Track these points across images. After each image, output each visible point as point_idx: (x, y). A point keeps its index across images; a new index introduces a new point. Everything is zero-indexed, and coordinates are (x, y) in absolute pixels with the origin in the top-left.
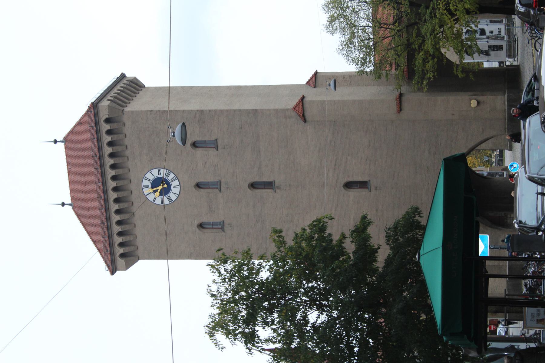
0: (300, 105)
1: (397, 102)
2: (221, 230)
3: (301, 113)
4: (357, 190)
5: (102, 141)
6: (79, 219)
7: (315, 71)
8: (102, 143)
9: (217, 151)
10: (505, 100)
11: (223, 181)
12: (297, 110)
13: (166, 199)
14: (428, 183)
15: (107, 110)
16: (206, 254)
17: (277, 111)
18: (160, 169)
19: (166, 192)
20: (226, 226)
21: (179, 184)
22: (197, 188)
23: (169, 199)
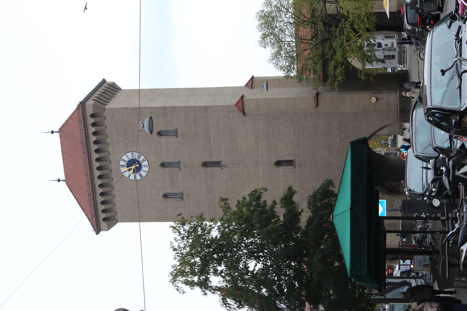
0: (241, 102)
1: (315, 100)
2: (180, 199)
4: (284, 167)
6: (72, 192)
7: (252, 76)
8: (89, 133)
9: (177, 138)
12: (238, 106)
14: (339, 161)
17: (222, 107)
18: (133, 152)
19: (138, 170)
20: (185, 196)
21: (148, 164)
22: (162, 167)
23: (141, 175)
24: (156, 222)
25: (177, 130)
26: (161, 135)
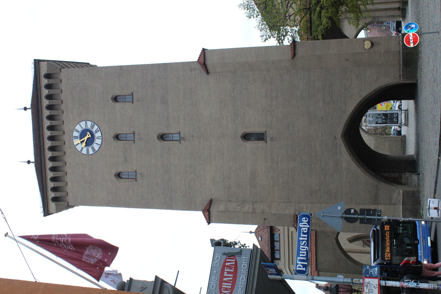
1: (291, 48)
2: (134, 180)
3: (202, 62)
4: (254, 142)
5: (41, 94)
8: (42, 96)
10: (400, 40)
13: (90, 149)
14: (322, 134)
15: (47, 66)
16: (121, 201)
20: (138, 175)
21: (101, 136)
22: (116, 139)
23: (93, 149)
25: (133, 94)
26: (117, 102)
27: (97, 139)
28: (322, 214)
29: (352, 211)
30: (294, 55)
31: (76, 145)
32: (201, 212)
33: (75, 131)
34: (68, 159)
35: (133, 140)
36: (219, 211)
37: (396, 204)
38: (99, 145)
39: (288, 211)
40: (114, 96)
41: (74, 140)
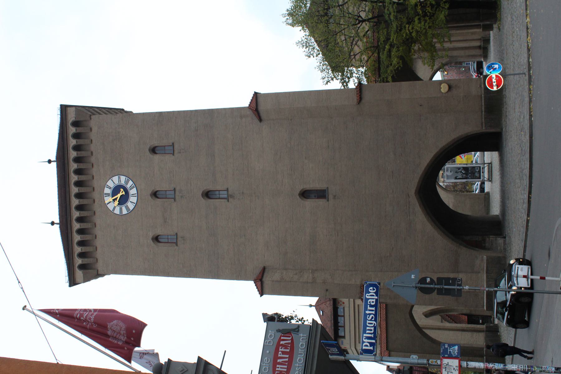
1: (357, 91)
3: (254, 108)
4: (314, 200)
8: (68, 147)
10: (481, 83)
11: (177, 189)
14: (393, 191)
16: (159, 269)
20: (179, 239)
21: (136, 193)
22: (154, 197)
23: (127, 208)
24: (143, 275)
25: (174, 144)
27: (131, 196)
28: (393, 284)
29: (428, 280)
30: (360, 99)
31: (107, 204)
32: (253, 282)
33: (106, 187)
34: (99, 220)
35: (173, 198)
36: (273, 281)
37: (479, 272)
38: (134, 203)
39: (353, 280)
40: (152, 147)
41: (105, 198)
